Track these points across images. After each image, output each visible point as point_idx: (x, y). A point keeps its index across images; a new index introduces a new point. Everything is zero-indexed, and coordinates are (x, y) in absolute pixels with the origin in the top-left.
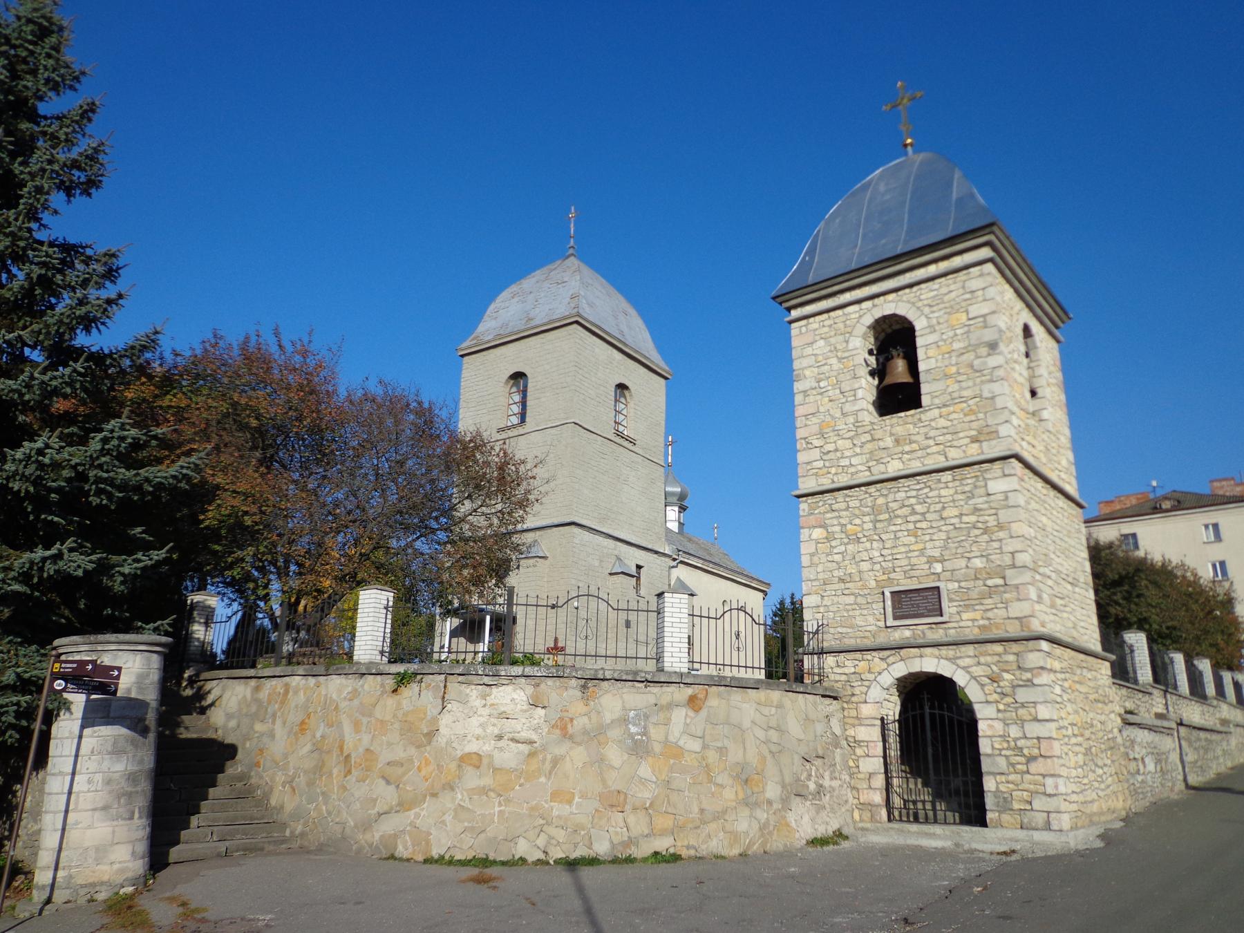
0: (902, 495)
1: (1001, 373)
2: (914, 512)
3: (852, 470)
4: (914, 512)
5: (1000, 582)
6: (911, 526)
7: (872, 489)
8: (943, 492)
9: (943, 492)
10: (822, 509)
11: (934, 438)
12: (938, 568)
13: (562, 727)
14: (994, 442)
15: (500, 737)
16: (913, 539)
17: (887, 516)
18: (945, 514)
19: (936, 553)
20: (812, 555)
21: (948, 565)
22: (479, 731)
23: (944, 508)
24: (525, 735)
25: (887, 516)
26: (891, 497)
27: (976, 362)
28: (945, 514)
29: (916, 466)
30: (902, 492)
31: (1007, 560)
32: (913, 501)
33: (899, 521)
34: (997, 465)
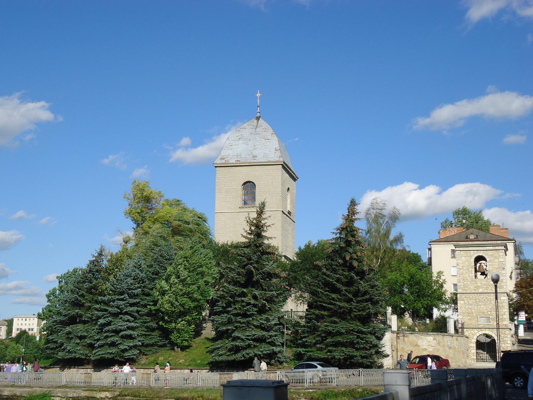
0: (482, 297)
1: (504, 275)
2: (485, 301)
3: (470, 289)
4: (485, 301)
5: (502, 317)
6: (484, 303)
7: (475, 294)
8: (491, 298)
9: (491, 298)
10: (463, 297)
11: (490, 286)
12: (489, 313)
13: (439, 343)
14: (502, 289)
15: (429, 345)
16: (484, 306)
17: (478, 301)
18: (491, 302)
19: (489, 310)
20: (461, 307)
21: (491, 313)
22: (425, 344)
23: (491, 301)
24: (433, 345)
25: (478, 301)
26: (480, 297)
27: (500, 271)
28: (491, 302)
29: (486, 291)
30: (482, 296)
31: (503, 313)
32: (485, 298)
33: (481, 302)
34: (503, 294)
